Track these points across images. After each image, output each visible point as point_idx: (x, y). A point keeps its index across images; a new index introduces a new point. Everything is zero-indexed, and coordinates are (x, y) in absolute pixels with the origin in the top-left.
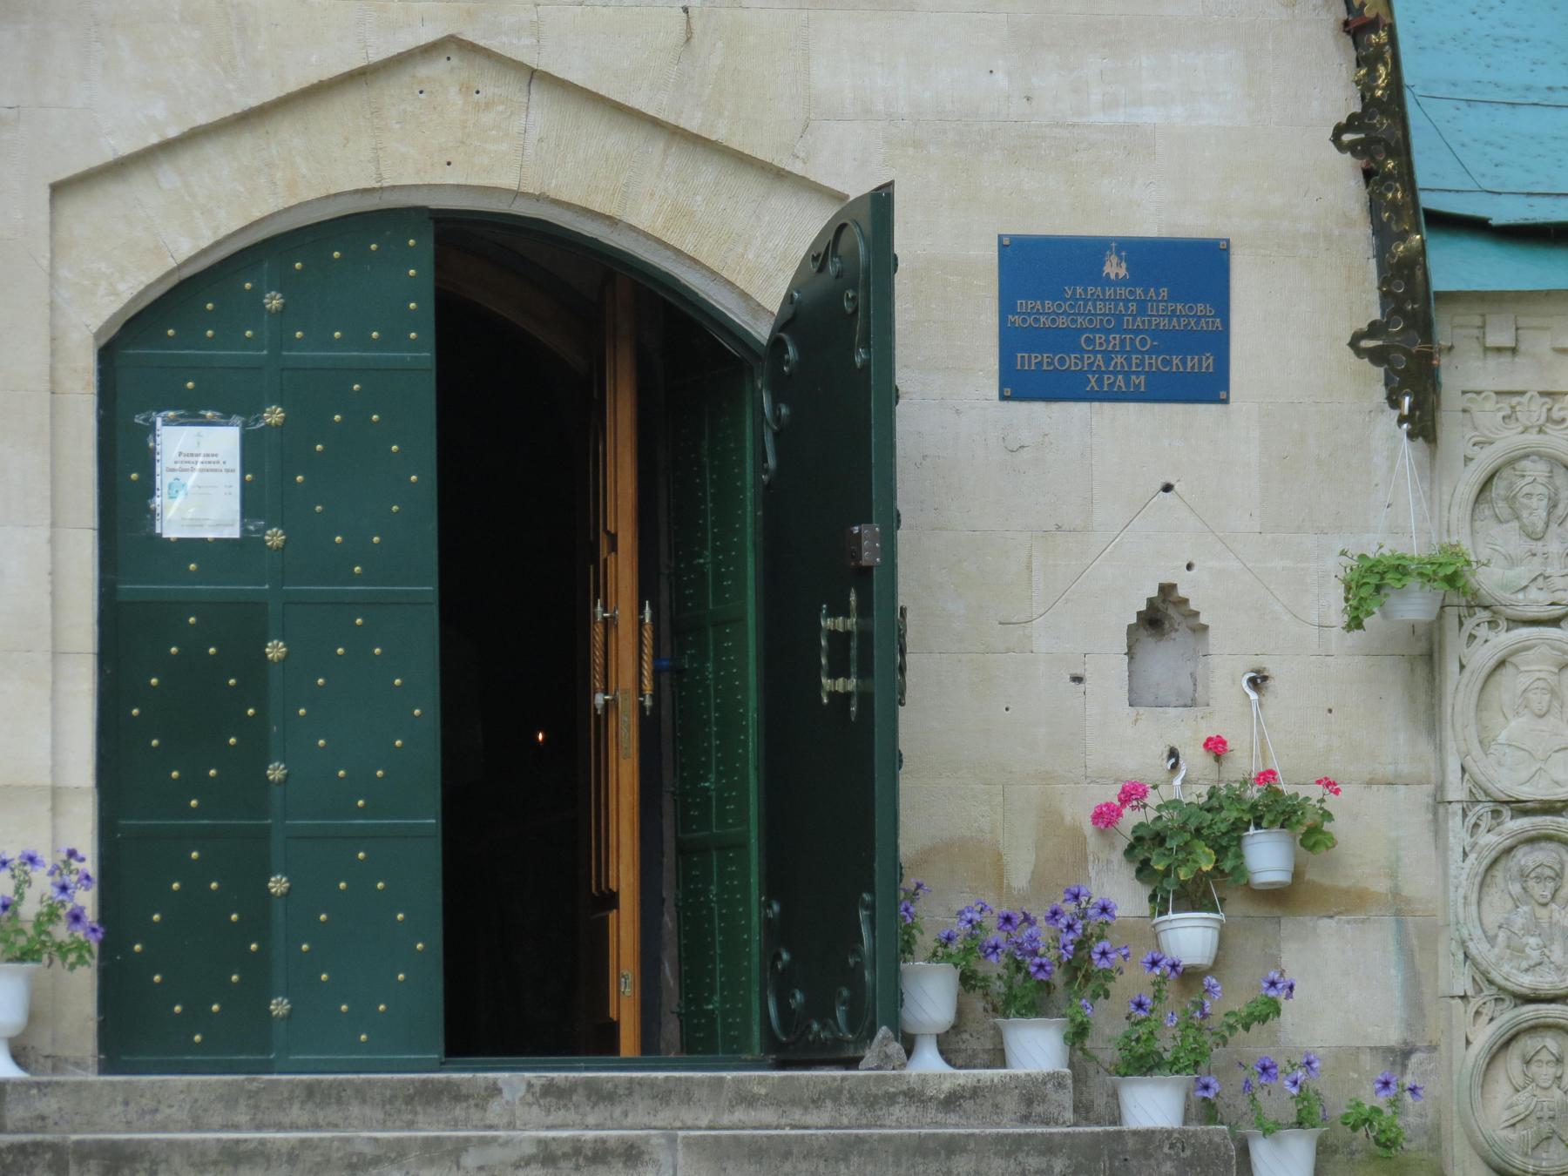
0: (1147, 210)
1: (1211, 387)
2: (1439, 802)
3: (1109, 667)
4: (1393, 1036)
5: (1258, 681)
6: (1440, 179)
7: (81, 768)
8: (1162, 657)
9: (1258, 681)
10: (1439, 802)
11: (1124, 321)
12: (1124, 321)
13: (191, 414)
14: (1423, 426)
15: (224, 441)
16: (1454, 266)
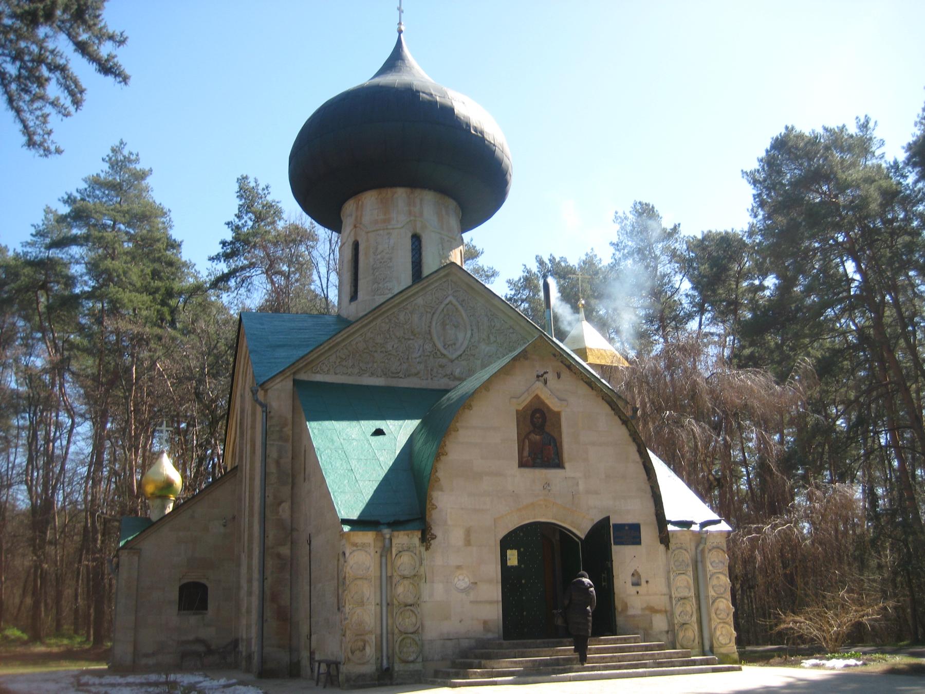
0: (630, 520)
1: (639, 543)
2: (671, 597)
3: (629, 580)
4: (666, 629)
5: (647, 582)
6: (668, 517)
7: (500, 599)
8: (635, 579)
9: (647, 582)
10: (671, 597)
11: (631, 534)
12: (631, 534)
13: (511, 549)
14: (667, 547)
15: (515, 552)
16: (670, 528)
